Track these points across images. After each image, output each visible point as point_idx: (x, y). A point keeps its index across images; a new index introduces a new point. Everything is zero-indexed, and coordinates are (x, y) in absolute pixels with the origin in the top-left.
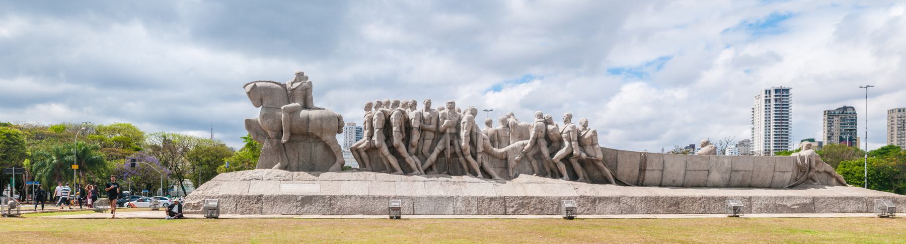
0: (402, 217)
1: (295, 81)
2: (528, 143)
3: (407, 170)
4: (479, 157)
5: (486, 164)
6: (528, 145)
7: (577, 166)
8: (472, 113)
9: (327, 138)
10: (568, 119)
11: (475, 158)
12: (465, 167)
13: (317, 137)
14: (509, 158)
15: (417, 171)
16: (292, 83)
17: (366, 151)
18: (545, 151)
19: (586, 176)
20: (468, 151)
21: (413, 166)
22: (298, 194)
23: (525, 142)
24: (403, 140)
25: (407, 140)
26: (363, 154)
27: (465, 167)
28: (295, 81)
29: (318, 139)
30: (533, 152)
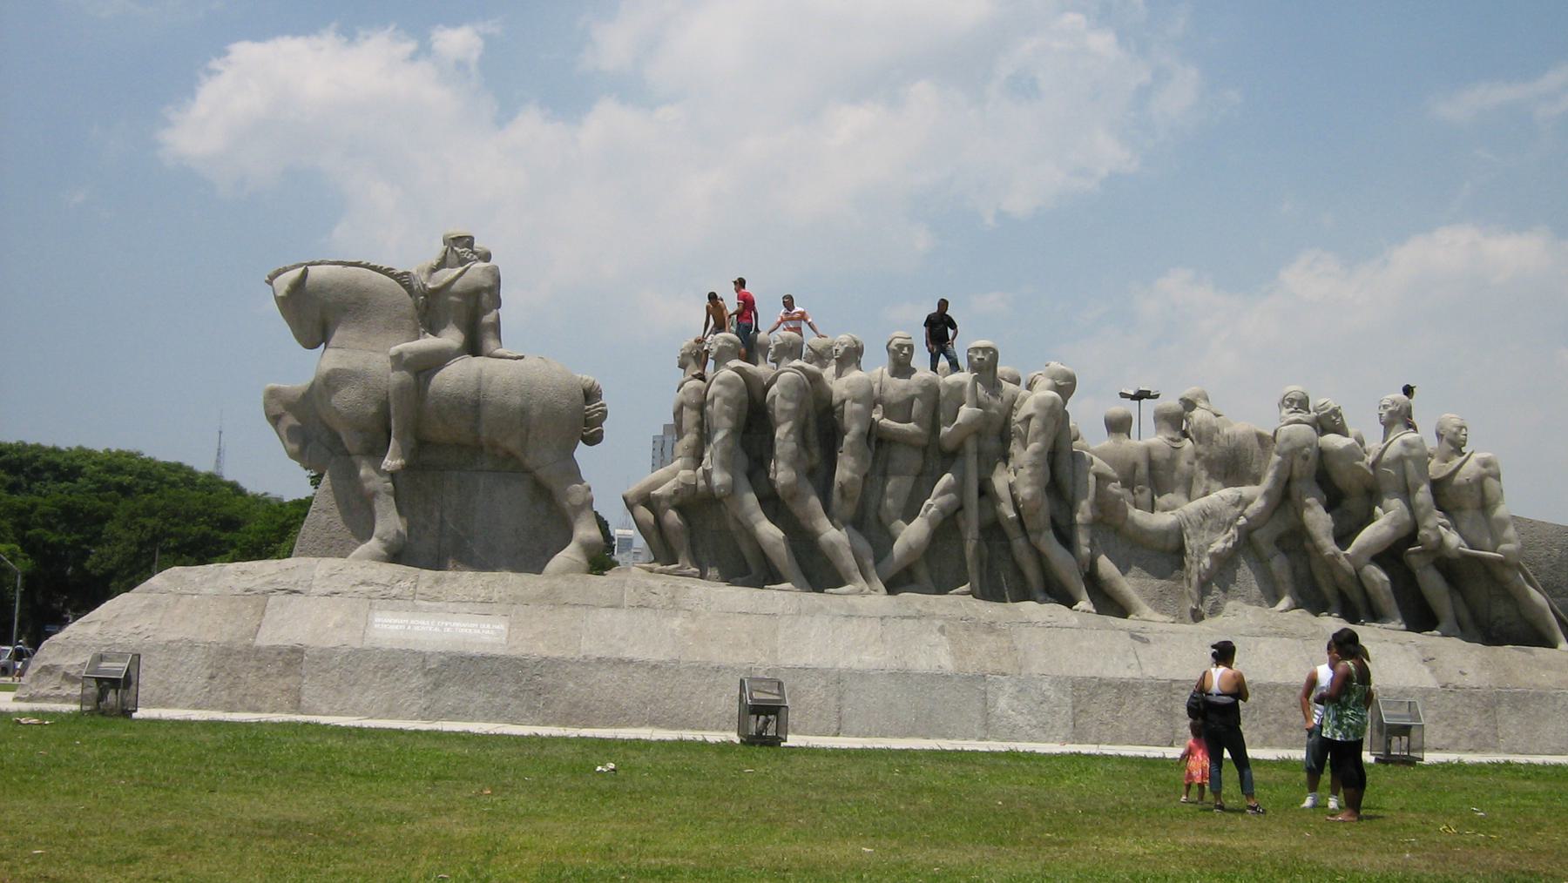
2: (1256, 495)
3: (819, 573)
4: (1083, 539)
5: (1106, 566)
6: (1259, 503)
7: (1433, 584)
8: (1057, 388)
10: (1401, 418)
11: (1066, 539)
12: (1031, 572)
13: (510, 455)
14: (1191, 543)
17: (680, 509)
18: (1318, 519)
19: (1465, 615)
20: (1044, 517)
21: (849, 561)
22: (428, 649)
23: (1247, 491)
24: (811, 473)
25: (820, 475)
26: (672, 516)
27: (1031, 572)
28: (443, 263)
29: (511, 465)
30: (1281, 525)
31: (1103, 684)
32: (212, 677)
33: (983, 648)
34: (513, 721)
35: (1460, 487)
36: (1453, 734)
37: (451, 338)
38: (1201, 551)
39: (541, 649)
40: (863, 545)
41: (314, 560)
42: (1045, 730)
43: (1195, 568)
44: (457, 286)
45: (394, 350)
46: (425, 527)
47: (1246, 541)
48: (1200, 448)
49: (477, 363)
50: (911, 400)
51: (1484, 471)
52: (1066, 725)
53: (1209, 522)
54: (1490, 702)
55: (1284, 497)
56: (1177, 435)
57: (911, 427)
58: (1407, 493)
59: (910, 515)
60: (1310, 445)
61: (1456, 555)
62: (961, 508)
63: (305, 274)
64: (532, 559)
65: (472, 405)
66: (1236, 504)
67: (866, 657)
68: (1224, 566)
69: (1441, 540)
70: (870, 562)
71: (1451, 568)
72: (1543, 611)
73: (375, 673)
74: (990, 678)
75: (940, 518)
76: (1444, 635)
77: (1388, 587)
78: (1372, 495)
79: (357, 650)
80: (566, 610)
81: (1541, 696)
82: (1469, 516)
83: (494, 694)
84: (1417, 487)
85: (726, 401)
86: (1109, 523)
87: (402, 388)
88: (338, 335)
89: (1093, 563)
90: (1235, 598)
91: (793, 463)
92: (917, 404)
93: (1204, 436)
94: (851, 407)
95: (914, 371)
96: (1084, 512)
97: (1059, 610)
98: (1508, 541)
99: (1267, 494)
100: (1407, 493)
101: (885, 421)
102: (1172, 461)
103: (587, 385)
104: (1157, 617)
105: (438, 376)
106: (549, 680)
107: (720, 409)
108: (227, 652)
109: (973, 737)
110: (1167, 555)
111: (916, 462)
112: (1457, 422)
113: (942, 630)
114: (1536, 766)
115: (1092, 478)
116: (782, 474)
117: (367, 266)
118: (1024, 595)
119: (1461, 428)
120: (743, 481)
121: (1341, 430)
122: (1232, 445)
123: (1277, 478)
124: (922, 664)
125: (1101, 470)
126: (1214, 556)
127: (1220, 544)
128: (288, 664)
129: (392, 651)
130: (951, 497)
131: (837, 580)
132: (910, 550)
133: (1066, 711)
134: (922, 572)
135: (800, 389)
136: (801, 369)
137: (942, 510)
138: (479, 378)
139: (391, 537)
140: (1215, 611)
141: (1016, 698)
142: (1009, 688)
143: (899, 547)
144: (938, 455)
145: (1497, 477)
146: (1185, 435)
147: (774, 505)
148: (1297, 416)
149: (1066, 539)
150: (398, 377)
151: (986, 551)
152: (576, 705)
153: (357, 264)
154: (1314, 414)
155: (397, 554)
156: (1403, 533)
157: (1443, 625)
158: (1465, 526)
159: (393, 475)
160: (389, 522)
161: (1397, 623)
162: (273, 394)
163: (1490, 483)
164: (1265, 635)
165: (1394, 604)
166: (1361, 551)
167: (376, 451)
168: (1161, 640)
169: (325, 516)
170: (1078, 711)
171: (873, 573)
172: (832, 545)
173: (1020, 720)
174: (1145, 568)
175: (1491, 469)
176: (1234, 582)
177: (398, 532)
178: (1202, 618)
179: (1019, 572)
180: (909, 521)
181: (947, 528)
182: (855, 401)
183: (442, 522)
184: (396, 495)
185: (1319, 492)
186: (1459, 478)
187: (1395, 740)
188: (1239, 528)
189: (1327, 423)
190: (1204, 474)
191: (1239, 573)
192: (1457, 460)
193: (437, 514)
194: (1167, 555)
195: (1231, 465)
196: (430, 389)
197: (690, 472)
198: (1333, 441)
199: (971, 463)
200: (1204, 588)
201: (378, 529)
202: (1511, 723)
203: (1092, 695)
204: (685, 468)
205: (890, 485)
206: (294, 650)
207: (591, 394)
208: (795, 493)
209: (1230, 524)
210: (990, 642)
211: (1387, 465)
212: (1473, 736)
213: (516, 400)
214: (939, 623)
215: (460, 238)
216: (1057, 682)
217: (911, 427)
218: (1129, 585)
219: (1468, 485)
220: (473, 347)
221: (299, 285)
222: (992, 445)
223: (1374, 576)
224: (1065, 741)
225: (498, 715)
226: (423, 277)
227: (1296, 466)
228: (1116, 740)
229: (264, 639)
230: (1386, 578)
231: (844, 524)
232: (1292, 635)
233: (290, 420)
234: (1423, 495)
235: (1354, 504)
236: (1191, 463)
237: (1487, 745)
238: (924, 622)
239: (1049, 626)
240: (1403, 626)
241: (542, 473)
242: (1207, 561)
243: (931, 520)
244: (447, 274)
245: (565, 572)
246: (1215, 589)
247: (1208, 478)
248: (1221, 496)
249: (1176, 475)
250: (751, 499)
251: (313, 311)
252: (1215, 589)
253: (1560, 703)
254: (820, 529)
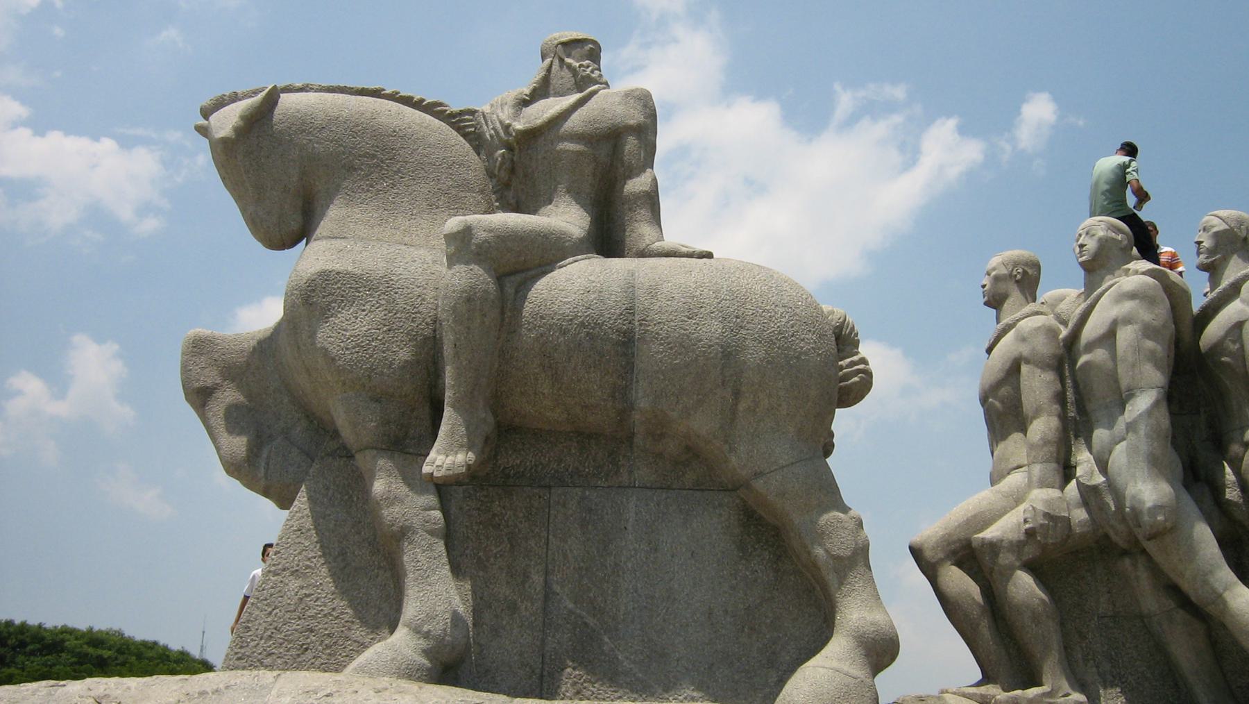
1: (542, 90)
9: (760, 455)
13: (692, 453)
16: (524, 103)
17: (1032, 568)
26: (1024, 586)
28: (542, 90)
29: (693, 472)
41: (267, 676)
44: (575, 122)
46: (513, 608)
63: (272, 99)
65: (617, 344)
85: (1148, 331)
87: (469, 300)
88: (334, 215)
107: (1138, 349)
117: (393, 97)
139: (439, 626)
153: (376, 93)
159: (442, 488)
160: (435, 594)
162: (199, 347)
167: (406, 443)
169: (294, 584)
177: (456, 618)
183: (548, 595)
184: (449, 535)
193: (537, 578)
196: (528, 308)
197: (1054, 493)
201: (411, 609)
204: (1043, 484)
213: (711, 329)
220: (607, 239)
221: (261, 117)
233: (230, 395)
250: (1204, 537)
251: (282, 172)
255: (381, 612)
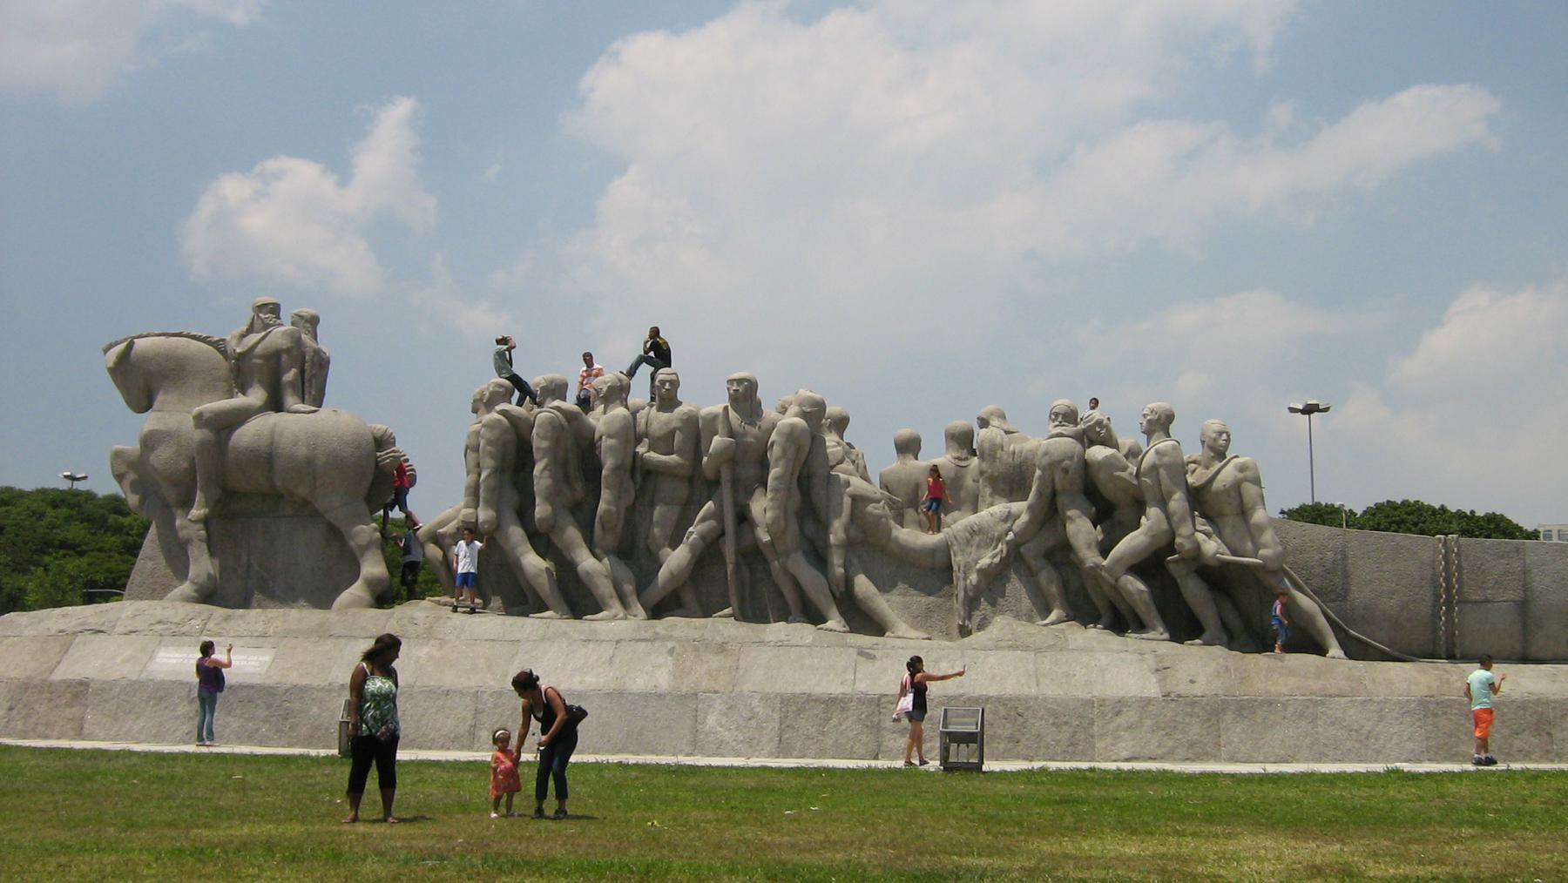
0: (989, 765)
1: (250, 330)
3: (578, 600)
6: (1024, 518)
7: (1194, 592)
11: (819, 558)
13: (305, 503)
14: (958, 560)
15: (616, 608)
16: (243, 336)
18: (1081, 530)
19: (1234, 621)
21: (604, 588)
28: (250, 330)
29: (307, 511)
30: (1048, 540)
31: (811, 699)
32: (11, 709)
33: (705, 667)
34: (261, 744)
35: (1218, 493)
36: (1170, 743)
37: (256, 396)
38: (968, 568)
39: (295, 678)
40: (625, 573)
42: (751, 745)
43: (961, 584)
44: (258, 350)
45: (196, 410)
47: (1014, 558)
48: (984, 466)
49: (273, 418)
50: (672, 433)
51: (1241, 475)
52: (772, 740)
53: (977, 539)
54: (1214, 711)
55: (1049, 514)
56: (964, 454)
57: (673, 458)
58: (1163, 503)
59: (675, 543)
60: (1071, 458)
61: (1212, 563)
62: (723, 534)
63: (130, 346)
64: (323, 599)
65: (266, 457)
66: (1005, 520)
67: (588, 679)
68: (993, 581)
69: (1198, 547)
70: (629, 588)
71: (1218, 577)
72: (1310, 618)
73: (147, 702)
74: (702, 696)
75: (701, 544)
76: (1206, 644)
77: (1146, 597)
78: (1140, 506)
79: (135, 682)
80: (329, 642)
81: (1270, 703)
82: (1230, 522)
83: (248, 720)
84: (1170, 494)
85: (489, 442)
86: (869, 544)
87: (203, 444)
88: (160, 399)
89: (848, 582)
90: (1003, 613)
91: (549, 498)
92: (678, 436)
93: (990, 453)
94: (607, 443)
95: (680, 403)
96: (837, 531)
97: (803, 632)
98: (1265, 546)
99: (1030, 508)
100: (1163, 503)
101: (653, 455)
102: (958, 480)
103: (379, 434)
104: (913, 633)
105: (238, 432)
106: (296, 705)
108: (26, 686)
109: (681, 752)
110: (933, 573)
111: (682, 491)
112: (1217, 427)
113: (671, 652)
114: (1138, 772)
115: (847, 501)
116: (541, 510)
118: (784, 616)
119: (1221, 433)
120: (510, 516)
121: (1109, 441)
122: (1017, 461)
123: (1040, 493)
124: (639, 683)
125: (860, 492)
126: (980, 571)
127: (986, 559)
128: (75, 696)
129: (162, 682)
130: (711, 523)
131: (595, 607)
132: (673, 577)
133: (773, 725)
134: (689, 597)
135: (554, 428)
136: (558, 409)
137: (703, 537)
138: (272, 433)
139: (203, 579)
140: (981, 627)
141: (725, 714)
142: (719, 705)
143: (663, 574)
144: (698, 483)
145: (1257, 481)
146: (973, 453)
147: (542, 541)
148: (1059, 430)
149: (819, 558)
150: (199, 435)
151: (747, 574)
152: (317, 728)
154: (1081, 426)
155: (208, 595)
156: (1163, 542)
157: (1206, 635)
158: (1227, 531)
160: (202, 565)
161: (1159, 632)
162: (117, 455)
163: (1249, 490)
164: (997, 648)
165: (1155, 613)
166: (1117, 561)
167: (187, 504)
168: (888, 655)
169: (150, 564)
170: (785, 726)
171: (633, 599)
172: (588, 573)
173: (727, 736)
174: (914, 586)
175: (1248, 473)
176: (1003, 596)
177: (209, 575)
178: (970, 633)
179: (779, 594)
180: (674, 546)
181: (707, 556)
182: (610, 436)
184: (209, 541)
185: (1086, 504)
186: (1218, 484)
187: (953, 746)
188: (1008, 543)
189: (1094, 436)
190: (988, 490)
191: (1009, 588)
192: (1218, 465)
194: (933, 573)
195: (1012, 482)
197: (471, 510)
198: (1098, 453)
199: (726, 490)
200: (971, 603)
201: (191, 574)
202: (1235, 731)
203: (799, 712)
204: (466, 506)
205: (658, 512)
206: (81, 683)
207: (382, 442)
208: (554, 525)
209: (999, 540)
210: (715, 661)
211: (1145, 475)
212: (1192, 745)
213: (302, 451)
214: (670, 645)
215: (265, 305)
216: (766, 698)
217: (673, 458)
218: (884, 604)
219: (1226, 491)
221: (125, 357)
222: (750, 472)
223: (1130, 587)
224: (770, 755)
225: (250, 739)
226: (234, 343)
227: (1057, 480)
228: (821, 754)
229: (57, 676)
230: (1142, 586)
231: (607, 553)
232: (1026, 648)
233: (132, 476)
234: (1178, 501)
235: (1123, 514)
236: (976, 481)
237: (1206, 754)
238: (657, 644)
239: (780, 644)
240: (1166, 636)
241: (330, 517)
242: (973, 578)
243: (693, 548)
244: (253, 338)
245: (356, 603)
246: (984, 604)
247: (991, 495)
248: (997, 509)
249: (962, 494)
251: (140, 379)
252: (984, 604)
253: (1291, 709)
254: (578, 559)
255: (181, 573)
